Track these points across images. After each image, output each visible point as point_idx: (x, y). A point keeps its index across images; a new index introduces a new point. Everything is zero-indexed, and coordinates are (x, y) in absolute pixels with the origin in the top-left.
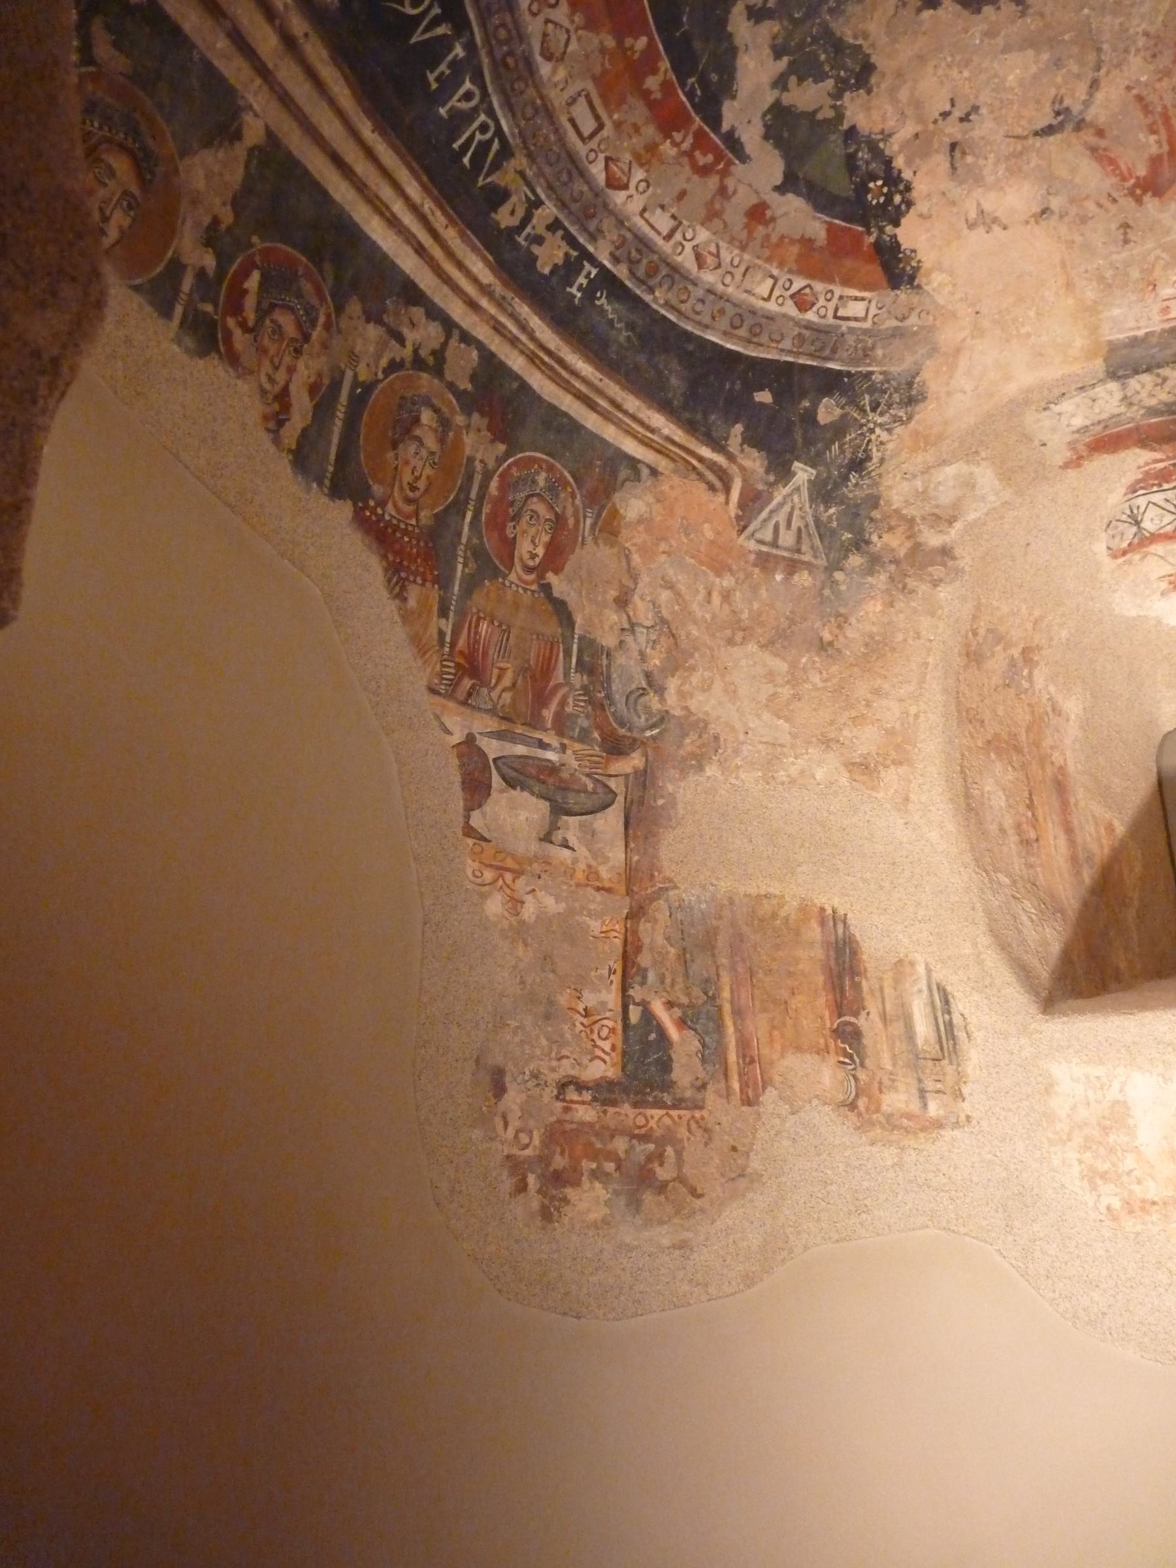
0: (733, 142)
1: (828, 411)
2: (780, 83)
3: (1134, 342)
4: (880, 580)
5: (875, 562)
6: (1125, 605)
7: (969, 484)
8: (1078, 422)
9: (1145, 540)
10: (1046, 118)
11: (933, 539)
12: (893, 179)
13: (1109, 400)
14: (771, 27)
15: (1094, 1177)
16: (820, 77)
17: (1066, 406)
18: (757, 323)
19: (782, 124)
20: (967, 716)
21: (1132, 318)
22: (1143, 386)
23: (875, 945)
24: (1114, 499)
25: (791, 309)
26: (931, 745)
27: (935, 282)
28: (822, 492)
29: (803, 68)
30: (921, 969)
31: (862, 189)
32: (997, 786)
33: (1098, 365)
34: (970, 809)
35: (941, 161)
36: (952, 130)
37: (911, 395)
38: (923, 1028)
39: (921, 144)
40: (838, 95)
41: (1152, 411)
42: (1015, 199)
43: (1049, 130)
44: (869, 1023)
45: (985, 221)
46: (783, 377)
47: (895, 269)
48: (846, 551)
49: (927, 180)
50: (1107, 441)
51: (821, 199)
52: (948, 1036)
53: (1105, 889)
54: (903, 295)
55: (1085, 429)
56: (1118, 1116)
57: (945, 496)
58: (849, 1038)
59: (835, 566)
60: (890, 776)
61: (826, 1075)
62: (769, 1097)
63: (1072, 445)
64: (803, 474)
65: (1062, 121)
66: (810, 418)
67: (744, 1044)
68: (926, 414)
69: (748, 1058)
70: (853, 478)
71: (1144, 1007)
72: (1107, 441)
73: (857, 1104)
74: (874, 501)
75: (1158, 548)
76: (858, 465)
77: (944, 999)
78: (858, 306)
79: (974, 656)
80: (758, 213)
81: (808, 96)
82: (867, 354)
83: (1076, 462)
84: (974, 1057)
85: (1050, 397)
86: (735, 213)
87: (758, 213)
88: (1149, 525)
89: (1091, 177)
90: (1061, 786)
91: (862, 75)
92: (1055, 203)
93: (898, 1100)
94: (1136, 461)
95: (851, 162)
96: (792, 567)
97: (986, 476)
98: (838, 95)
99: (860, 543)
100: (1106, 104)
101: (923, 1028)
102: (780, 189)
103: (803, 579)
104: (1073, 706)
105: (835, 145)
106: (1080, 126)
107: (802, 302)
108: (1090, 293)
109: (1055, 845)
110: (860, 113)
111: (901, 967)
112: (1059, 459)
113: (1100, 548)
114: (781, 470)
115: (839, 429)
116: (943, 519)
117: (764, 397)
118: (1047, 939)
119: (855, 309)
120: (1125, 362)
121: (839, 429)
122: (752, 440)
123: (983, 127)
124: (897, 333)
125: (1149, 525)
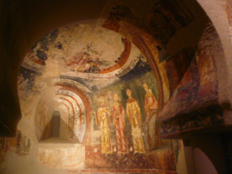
0: (33, 52)
1: (32, 74)
2: (40, 48)
3: (63, 76)
4: (32, 93)
5: (32, 91)
6: (55, 99)
7: (44, 85)
8: (56, 81)
9: (58, 94)
10: (62, 57)
11: (39, 90)
12: (46, 57)
13: (59, 80)
14: (40, 45)
15: (41, 160)
16: (43, 49)
17: (55, 79)
18: (28, 65)
19: (38, 52)
20: (37, 109)
21: (63, 74)
22: (62, 80)
23: (23, 135)
24: (57, 90)
25: (32, 65)
26: (34, 113)
27: (47, 66)
28: (29, 82)
29: (42, 47)
30: (27, 137)
31: (43, 57)
32: (38, 118)
33: (59, 76)
34: (36, 120)
35: (51, 57)
36: (53, 56)
37: (41, 74)
38: (26, 144)
39: (50, 56)
40: (44, 50)
41: (63, 83)
42: (57, 62)
43: (62, 59)
44: (21, 143)
45: (53, 63)
46: (29, 71)
47: (44, 64)
48: (29, 89)
49: (49, 58)
50: (58, 84)
51: (39, 57)
52: (29, 145)
53: (46, 129)
54: (43, 66)
55: (56, 82)
56: (44, 154)
57: (41, 85)
58: (18, 145)
59: (28, 91)
60: (29, 116)
61: (15, 149)
62: (8, 151)
63: (55, 84)
64: (27, 80)
65: (63, 58)
66: (30, 75)
67: (7, 145)
68: (42, 77)
69: (7, 147)
70: (32, 81)
71: (48, 142)
72: (58, 84)
73: (18, 152)
74: (34, 84)
75: (59, 95)
76: (33, 80)
77: (29, 141)
78: (38, 66)
79: (40, 103)
80: (33, 57)
81: (42, 50)
82: (38, 70)
83: (54, 86)
84: (31, 147)
85: (54, 78)
86: (30, 57)
87: (33, 57)
88: (59, 92)
89: (64, 63)
90: (44, 117)
91: (47, 50)
92: (60, 63)
93: (22, 152)
94: (60, 87)
95: (43, 55)
96: (23, 90)
97: (46, 84)
98: (44, 50)
99: (31, 89)
100: (67, 59)
101: (26, 144)
102: (36, 55)
103: (24, 92)
104: (47, 108)
105: (43, 53)
106: (64, 59)
107: (33, 64)
108: (60, 70)
109: (42, 124)
110: (46, 52)
111: (25, 137)
112: (53, 84)
113: (54, 93)
114: (25, 79)
115: (32, 76)
116: (40, 88)
117: (26, 72)
118: (40, 134)
119: (38, 66)
120: (61, 77)
121: (32, 76)
122: (23, 76)
123: (56, 56)
124: (41, 69)
125: (59, 92)
